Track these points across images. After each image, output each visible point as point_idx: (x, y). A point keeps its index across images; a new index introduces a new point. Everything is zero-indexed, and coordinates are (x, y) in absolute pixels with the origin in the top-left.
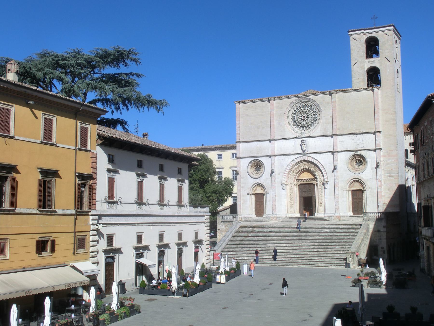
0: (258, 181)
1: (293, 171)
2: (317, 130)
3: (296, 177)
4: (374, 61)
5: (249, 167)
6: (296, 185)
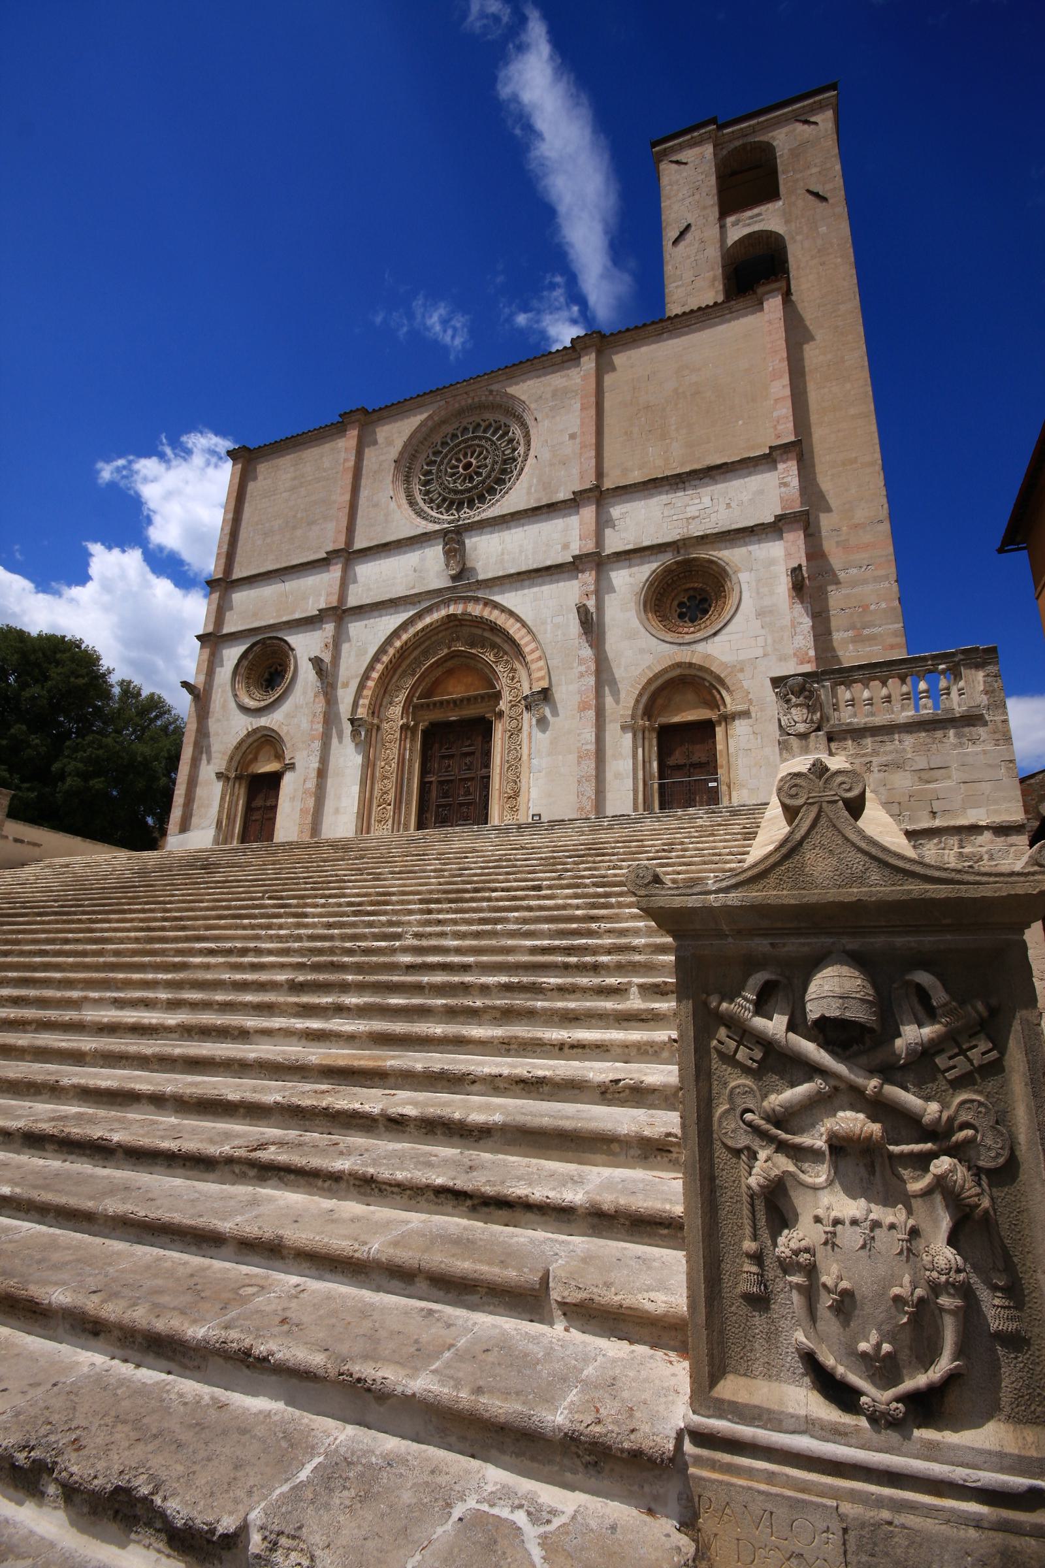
0: (263, 721)
1: (405, 671)
2: (516, 497)
3: (417, 695)
4: (759, 214)
5: (242, 670)
6: (413, 730)
